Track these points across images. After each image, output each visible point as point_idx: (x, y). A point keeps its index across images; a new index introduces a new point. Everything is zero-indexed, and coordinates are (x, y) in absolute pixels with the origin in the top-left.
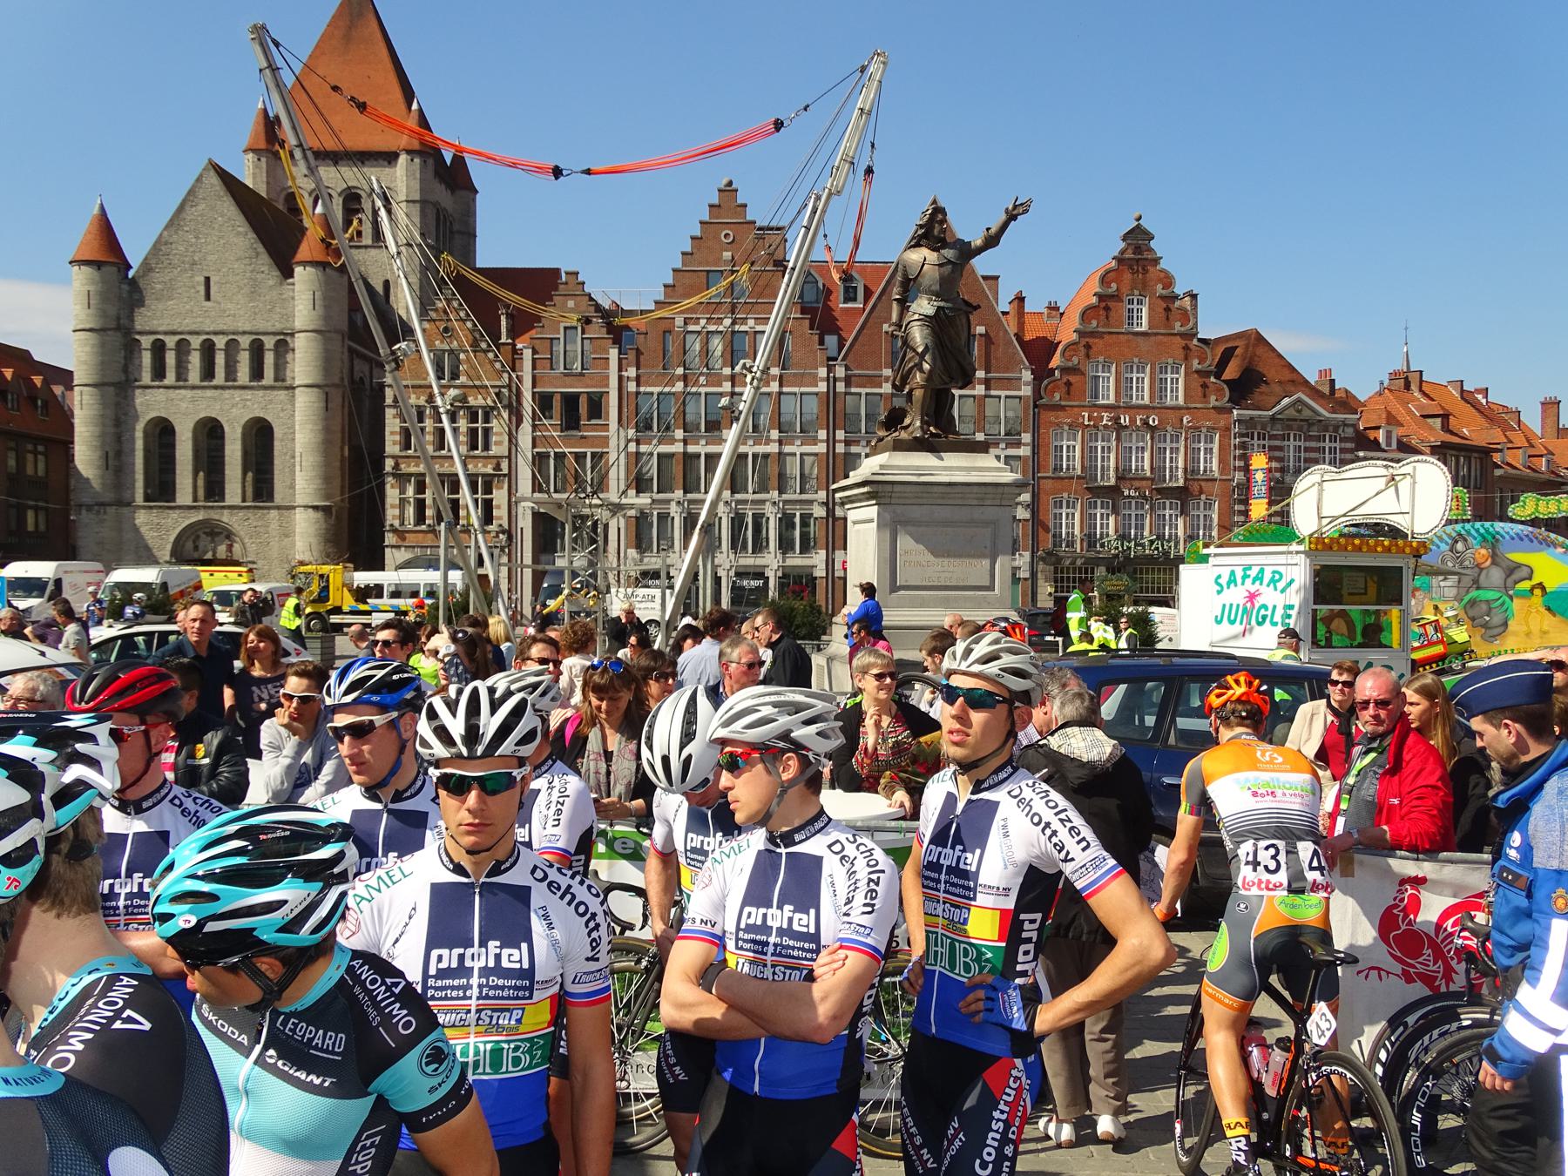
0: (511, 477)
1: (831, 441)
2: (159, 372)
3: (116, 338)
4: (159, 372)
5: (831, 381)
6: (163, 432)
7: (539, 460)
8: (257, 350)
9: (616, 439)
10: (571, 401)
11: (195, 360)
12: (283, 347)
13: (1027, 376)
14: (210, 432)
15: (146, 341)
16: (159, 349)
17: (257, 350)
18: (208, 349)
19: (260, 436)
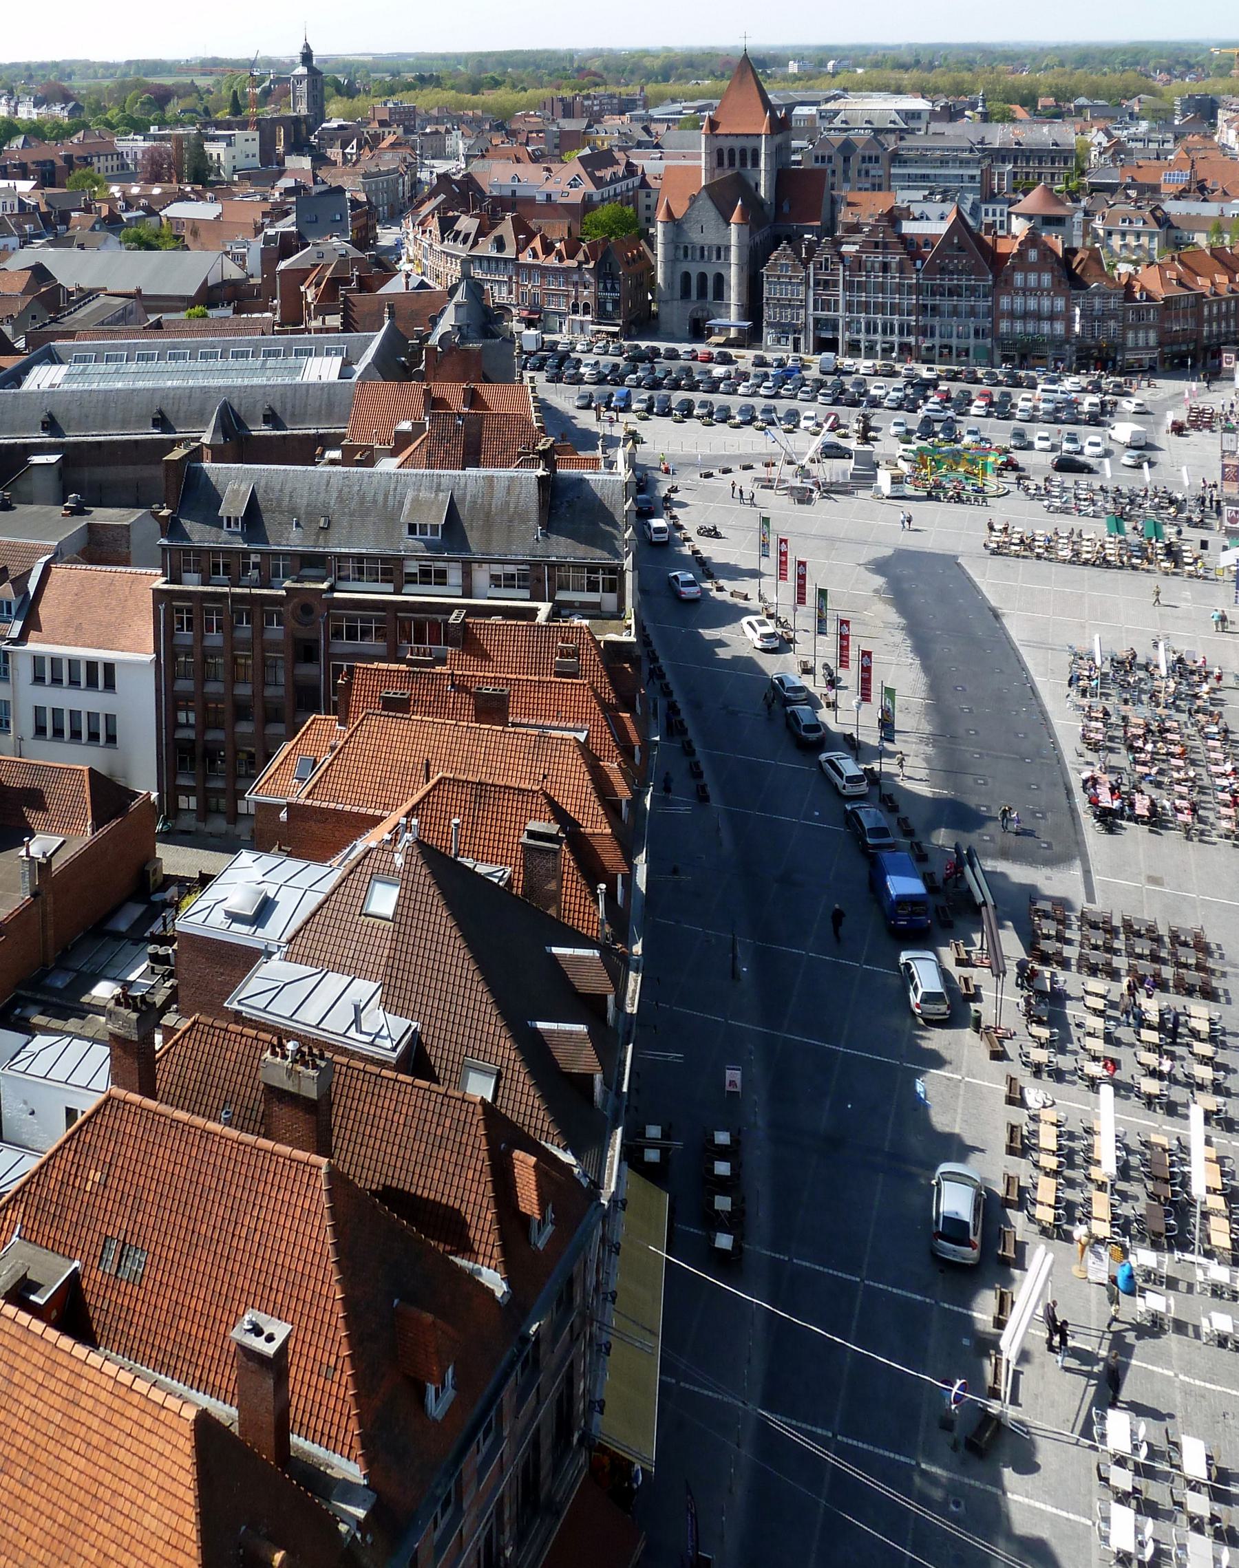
0: (806, 307)
1: (917, 300)
2: (686, 255)
3: (671, 246)
4: (686, 255)
5: (918, 279)
6: (686, 276)
7: (815, 301)
8: (719, 250)
9: (841, 295)
10: (826, 282)
11: (698, 252)
12: (728, 248)
13: (990, 277)
14: (703, 277)
15: (682, 246)
16: (686, 248)
17: (719, 250)
18: (702, 248)
19: (720, 280)
